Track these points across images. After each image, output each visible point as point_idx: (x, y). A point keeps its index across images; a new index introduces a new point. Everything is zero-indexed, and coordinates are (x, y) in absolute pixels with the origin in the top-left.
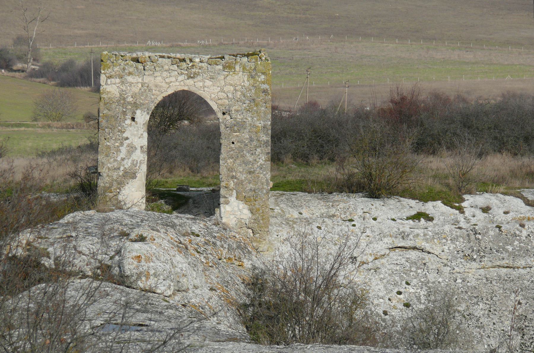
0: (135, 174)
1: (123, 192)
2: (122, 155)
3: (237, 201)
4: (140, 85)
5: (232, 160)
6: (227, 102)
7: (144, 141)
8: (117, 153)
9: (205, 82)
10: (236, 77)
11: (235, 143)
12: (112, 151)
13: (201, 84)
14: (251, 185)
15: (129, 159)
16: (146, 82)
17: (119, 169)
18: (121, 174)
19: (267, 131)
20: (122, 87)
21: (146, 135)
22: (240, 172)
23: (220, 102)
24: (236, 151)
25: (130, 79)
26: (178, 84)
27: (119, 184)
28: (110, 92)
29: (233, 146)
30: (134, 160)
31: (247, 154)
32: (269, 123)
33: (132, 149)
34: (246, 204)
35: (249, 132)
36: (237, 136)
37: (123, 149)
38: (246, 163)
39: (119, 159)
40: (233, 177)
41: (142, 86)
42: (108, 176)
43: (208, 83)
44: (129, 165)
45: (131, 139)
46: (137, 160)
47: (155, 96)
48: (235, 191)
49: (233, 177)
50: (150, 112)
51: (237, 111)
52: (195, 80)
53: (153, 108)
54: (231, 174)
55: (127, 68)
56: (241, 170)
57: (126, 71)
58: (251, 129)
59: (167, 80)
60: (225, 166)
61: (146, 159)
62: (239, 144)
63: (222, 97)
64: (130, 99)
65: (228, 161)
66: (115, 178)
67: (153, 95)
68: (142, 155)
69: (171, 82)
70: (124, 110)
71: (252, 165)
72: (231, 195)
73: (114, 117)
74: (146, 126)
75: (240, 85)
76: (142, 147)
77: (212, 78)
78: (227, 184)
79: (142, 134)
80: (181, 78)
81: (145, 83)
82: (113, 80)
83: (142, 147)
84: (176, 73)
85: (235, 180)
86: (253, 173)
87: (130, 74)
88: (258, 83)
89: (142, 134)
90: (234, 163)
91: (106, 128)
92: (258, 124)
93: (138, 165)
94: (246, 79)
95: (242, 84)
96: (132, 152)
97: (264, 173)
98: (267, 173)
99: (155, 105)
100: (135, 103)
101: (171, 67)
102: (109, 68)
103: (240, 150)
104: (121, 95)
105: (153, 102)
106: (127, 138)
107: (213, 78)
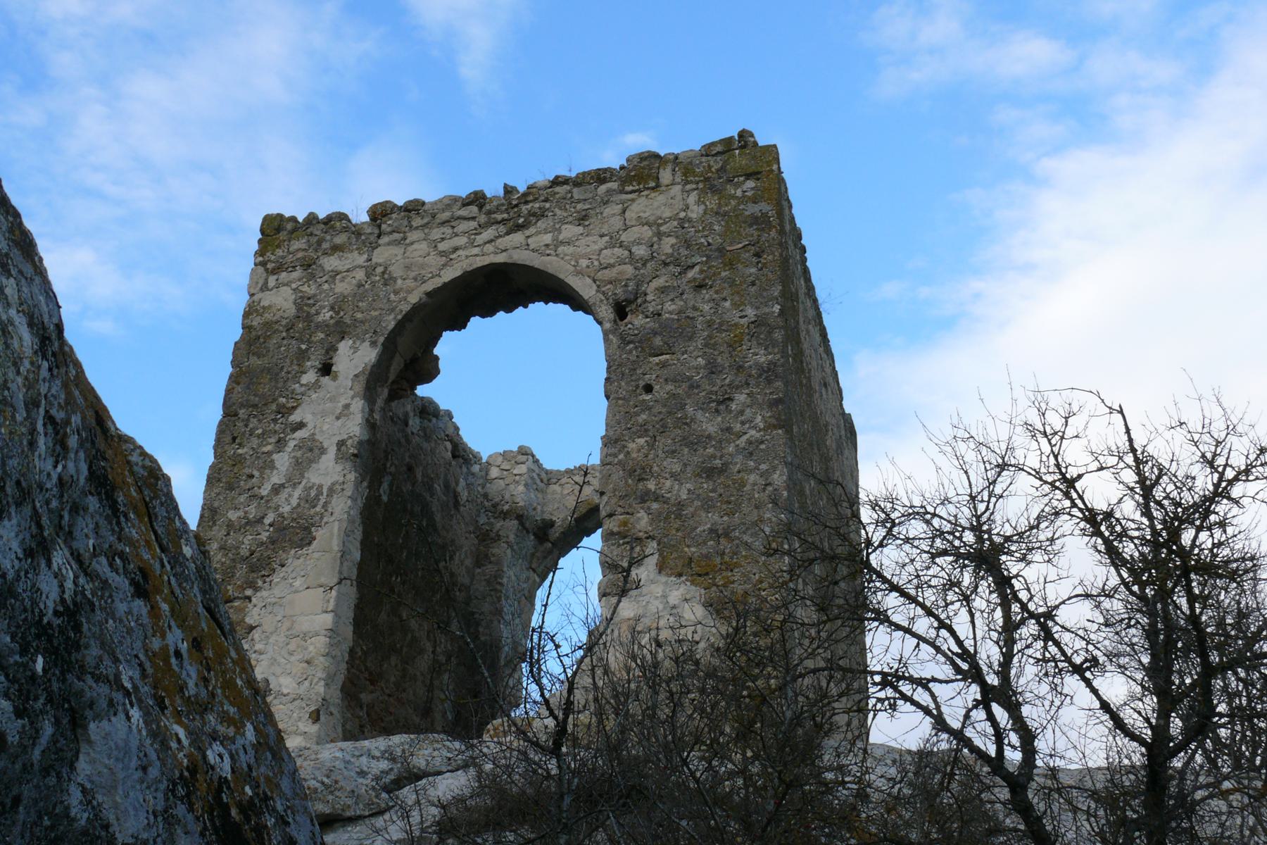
0: (307, 529)
1: (264, 593)
2: (276, 479)
3: (663, 579)
4: (360, 275)
5: (641, 441)
6: (629, 270)
7: (354, 427)
8: (262, 474)
9: (559, 230)
10: (660, 199)
11: (657, 387)
12: (247, 471)
13: (548, 238)
14: (714, 517)
15: (295, 486)
16: (380, 261)
17: (260, 520)
18: (264, 536)
19: (770, 333)
20: (305, 288)
21: (358, 405)
22: (673, 475)
23: (607, 275)
24: (658, 408)
25: (331, 263)
26: (476, 251)
27: (253, 569)
28: (270, 307)
29: (648, 397)
30: (311, 488)
31: (699, 415)
32: (777, 308)
34: (693, 583)
35: (706, 345)
36: (664, 365)
37: (283, 461)
38: (694, 442)
39: (264, 492)
40: (645, 497)
42: (221, 548)
43: (570, 231)
44: (294, 502)
45: (310, 426)
46: (321, 486)
47: (402, 295)
48: (652, 546)
49: (645, 497)
50: (382, 339)
51: (663, 290)
52: (532, 230)
53: (392, 325)
54: (640, 486)
55: (328, 238)
56: (677, 468)
57: (325, 245)
58: (710, 337)
59: (441, 246)
60: (620, 462)
61: (352, 477)
62: (670, 387)
63: (612, 261)
64: (326, 315)
65: (631, 446)
66: (244, 552)
67: (396, 293)
68: (339, 468)
69: (456, 249)
70: (304, 347)
71: (720, 445)
73: (269, 370)
74: (363, 379)
75: (674, 217)
76: (341, 444)
77: (582, 219)
78: (625, 524)
79: (347, 406)
81: (378, 265)
82: (284, 274)
83: (341, 444)
84: (473, 224)
85: (655, 506)
87: (336, 249)
88: (733, 203)
90: (651, 446)
91: (242, 406)
93: (323, 499)
94: (692, 198)
95: (682, 215)
96: (311, 461)
97: (763, 467)
98: (774, 468)
99: (400, 317)
100: (338, 323)
102: (278, 246)
103: (675, 403)
104: (299, 308)
105: (393, 310)
106: (301, 425)
107: (585, 218)
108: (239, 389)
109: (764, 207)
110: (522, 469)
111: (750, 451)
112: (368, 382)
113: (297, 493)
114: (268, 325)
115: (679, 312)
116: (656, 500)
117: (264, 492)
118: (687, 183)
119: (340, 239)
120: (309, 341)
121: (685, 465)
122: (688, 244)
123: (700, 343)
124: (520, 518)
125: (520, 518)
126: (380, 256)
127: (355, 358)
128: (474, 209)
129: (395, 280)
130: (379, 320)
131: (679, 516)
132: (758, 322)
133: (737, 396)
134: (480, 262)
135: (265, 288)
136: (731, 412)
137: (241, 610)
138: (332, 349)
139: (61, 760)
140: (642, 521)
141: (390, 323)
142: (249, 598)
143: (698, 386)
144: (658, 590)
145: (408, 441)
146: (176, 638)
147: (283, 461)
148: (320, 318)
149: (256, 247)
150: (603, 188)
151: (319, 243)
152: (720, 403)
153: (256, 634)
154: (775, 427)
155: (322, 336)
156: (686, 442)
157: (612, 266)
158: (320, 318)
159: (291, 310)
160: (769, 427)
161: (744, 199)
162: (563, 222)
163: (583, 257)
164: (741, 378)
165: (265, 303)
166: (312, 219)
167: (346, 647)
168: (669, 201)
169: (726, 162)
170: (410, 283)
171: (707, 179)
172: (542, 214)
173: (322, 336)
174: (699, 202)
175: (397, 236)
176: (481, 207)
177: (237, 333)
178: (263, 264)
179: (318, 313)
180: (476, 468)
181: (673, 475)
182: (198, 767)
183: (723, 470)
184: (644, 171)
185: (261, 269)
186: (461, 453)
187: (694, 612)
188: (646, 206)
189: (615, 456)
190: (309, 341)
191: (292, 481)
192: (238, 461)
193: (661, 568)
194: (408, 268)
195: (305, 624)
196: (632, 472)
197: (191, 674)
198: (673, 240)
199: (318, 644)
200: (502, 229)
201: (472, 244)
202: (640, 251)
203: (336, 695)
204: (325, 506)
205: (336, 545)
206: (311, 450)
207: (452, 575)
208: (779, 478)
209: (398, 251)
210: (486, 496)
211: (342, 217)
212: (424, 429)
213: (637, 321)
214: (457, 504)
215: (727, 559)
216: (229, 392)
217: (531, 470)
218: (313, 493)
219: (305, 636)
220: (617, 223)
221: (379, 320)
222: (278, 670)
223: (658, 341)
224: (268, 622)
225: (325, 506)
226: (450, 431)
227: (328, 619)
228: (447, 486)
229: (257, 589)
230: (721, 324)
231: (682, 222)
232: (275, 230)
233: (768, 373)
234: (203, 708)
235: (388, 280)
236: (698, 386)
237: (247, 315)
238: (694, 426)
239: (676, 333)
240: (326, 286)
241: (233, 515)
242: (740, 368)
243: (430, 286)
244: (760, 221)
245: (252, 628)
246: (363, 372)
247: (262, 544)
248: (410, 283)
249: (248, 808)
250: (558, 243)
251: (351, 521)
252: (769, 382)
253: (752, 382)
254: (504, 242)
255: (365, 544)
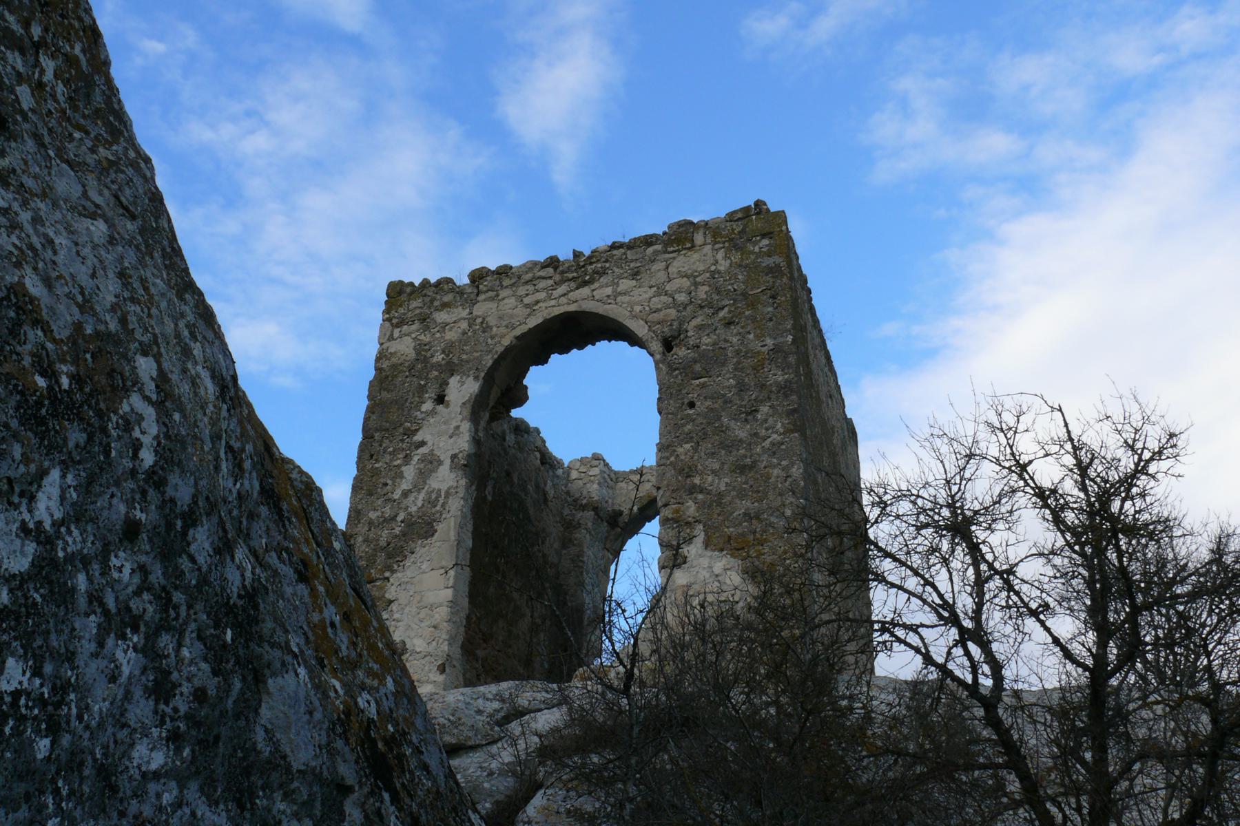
0: (430, 524)
1: (399, 575)
2: (405, 486)
3: (709, 553)
5: (688, 446)
6: (673, 313)
7: (463, 443)
8: (394, 482)
9: (618, 285)
10: (696, 256)
11: (698, 404)
12: (382, 480)
13: (609, 291)
15: (419, 491)
17: (393, 518)
18: (397, 531)
20: (422, 337)
21: (466, 426)
22: (714, 472)
24: (700, 420)
25: (441, 317)
26: (553, 303)
27: (390, 556)
28: (395, 353)
29: (691, 412)
32: (790, 338)
33: (431, 463)
34: (732, 556)
35: (736, 369)
36: (703, 386)
37: (409, 472)
38: (729, 445)
40: (693, 490)
41: (470, 325)
42: (365, 541)
43: (625, 284)
44: (420, 503)
45: (430, 444)
46: (439, 490)
49: (693, 490)
50: (482, 374)
51: (700, 328)
52: (596, 285)
53: (490, 363)
56: (716, 466)
57: (436, 303)
58: (739, 363)
61: (463, 482)
62: (708, 403)
64: (439, 357)
65: (680, 450)
66: (383, 543)
67: (492, 338)
68: (453, 476)
69: (537, 302)
72: (689, 540)
73: (396, 402)
74: (469, 406)
77: (635, 274)
78: (677, 511)
79: (458, 427)
80: (562, 289)
83: (454, 457)
84: (550, 282)
85: (700, 497)
86: (752, 467)
87: (445, 305)
88: (753, 257)
89: (458, 427)
90: (695, 449)
91: (377, 430)
92: (756, 346)
93: (441, 501)
94: (720, 255)
95: (713, 268)
96: (432, 471)
97: (784, 463)
98: (793, 464)
100: (450, 363)
101: (542, 273)
102: (401, 306)
106: (422, 444)
107: (637, 273)
108: (374, 417)
109: (777, 259)
110: (596, 471)
111: (774, 450)
112: (473, 407)
113: (422, 496)
114: (394, 367)
115: (714, 345)
116: (701, 492)
117: (396, 497)
118: (716, 243)
119: (448, 298)
120: (426, 378)
121: (723, 464)
122: (718, 291)
123: (731, 367)
124: (595, 509)
125: (595, 509)
126: (479, 310)
127: (462, 390)
128: (550, 270)
129: (491, 327)
130: (480, 359)
131: (719, 504)
132: (776, 349)
133: (761, 408)
134: (557, 311)
135: (391, 338)
136: (757, 420)
137: (382, 588)
138: (445, 383)
139: (248, 707)
140: (691, 509)
141: (488, 361)
142: (388, 579)
143: (731, 402)
144: (705, 562)
145: (506, 453)
146: (331, 613)
147: (409, 472)
148: (434, 360)
149: (383, 307)
150: (650, 250)
151: (432, 302)
152: (748, 414)
153: (394, 607)
154: (792, 431)
155: (436, 373)
156: (723, 445)
157: (660, 310)
158: (434, 360)
159: (412, 354)
160: (787, 431)
161: (759, 255)
162: (620, 277)
163: (638, 303)
164: (765, 394)
165: (392, 350)
166: (425, 283)
167: (463, 614)
168: (703, 258)
169: (745, 226)
170: (503, 330)
171: (731, 240)
172: (602, 273)
173: (436, 373)
174: (725, 258)
175: (491, 294)
176: (556, 268)
177: (371, 374)
178: (389, 320)
179: (432, 356)
180: (560, 472)
181: (714, 472)
182: (351, 710)
183: (752, 467)
184: (682, 236)
185: (388, 324)
186: (548, 461)
187: (735, 578)
188: (685, 262)
189: (668, 458)
190: (426, 378)
191: (417, 487)
192: (376, 473)
193: (707, 545)
194: (500, 318)
195: (431, 598)
196: (681, 471)
197: (343, 640)
198: (706, 288)
199: (442, 613)
200: (573, 285)
201: (550, 297)
202: (682, 298)
203: (457, 652)
204: (443, 505)
205: (453, 535)
206: (431, 463)
207: (544, 556)
208: (797, 471)
209: (493, 305)
210: (568, 493)
211: (449, 281)
212: (518, 443)
213: (681, 352)
214: (546, 500)
215: (758, 536)
216: (366, 420)
217: (602, 472)
218: (434, 496)
219: (432, 607)
220: (662, 276)
221: (480, 359)
222: (413, 634)
223: (698, 367)
224: (403, 597)
225: (443, 505)
226: (539, 443)
227: (450, 592)
228: (537, 486)
229: (393, 572)
230: (746, 353)
231: (713, 274)
232: (398, 293)
233: (785, 389)
234: (354, 665)
235: (486, 328)
236: (731, 402)
237: (378, 359)
238: (729, 433)
239: (712, 360)
240: (438, 335)
241: (373, 515)
242: (763, 386)
243: (518, 332)
244: (774, 271)
245: (391, 602)
246: (469, 401)
247: (396, 536)
248: (503, 330)
249: (391, 741)
250: (617, 294)
251: (464, 517)
252: (786, 396)
253: (773, 396)
254: (572, 295)
255: (476, 535)
